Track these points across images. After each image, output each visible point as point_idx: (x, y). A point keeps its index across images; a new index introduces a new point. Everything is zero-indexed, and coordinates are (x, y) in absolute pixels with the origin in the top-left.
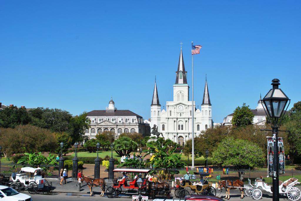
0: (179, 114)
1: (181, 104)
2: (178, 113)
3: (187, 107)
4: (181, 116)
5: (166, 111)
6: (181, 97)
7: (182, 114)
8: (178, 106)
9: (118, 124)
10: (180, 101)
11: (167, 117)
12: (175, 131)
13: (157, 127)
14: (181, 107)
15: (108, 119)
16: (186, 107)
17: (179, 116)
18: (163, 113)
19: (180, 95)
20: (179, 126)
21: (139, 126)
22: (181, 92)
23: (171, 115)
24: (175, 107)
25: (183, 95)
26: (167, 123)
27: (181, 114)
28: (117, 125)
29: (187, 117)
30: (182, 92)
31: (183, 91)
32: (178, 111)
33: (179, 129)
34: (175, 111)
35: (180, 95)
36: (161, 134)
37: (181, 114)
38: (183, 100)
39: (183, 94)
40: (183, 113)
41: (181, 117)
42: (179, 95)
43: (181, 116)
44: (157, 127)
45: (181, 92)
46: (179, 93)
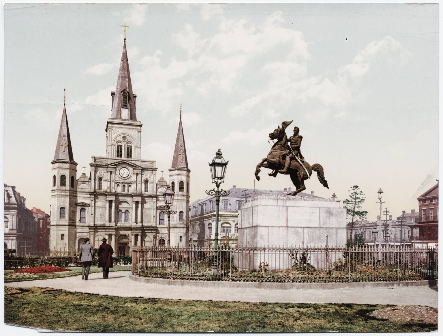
1: (124, 166)
2: (117, 184)
3: (139, 172)
4: (124, 190)
7: (127, 185)
13: (296, 131)
14: (124, 172)
24: (113, 170)
26: (93, 205)
27: (124, 186)
32: (117, 179)
37: (124, 186)
39: (129, 142)
40: (130, 184)
41: (126, 192)
42: (119, 144)
44: (296, 131)
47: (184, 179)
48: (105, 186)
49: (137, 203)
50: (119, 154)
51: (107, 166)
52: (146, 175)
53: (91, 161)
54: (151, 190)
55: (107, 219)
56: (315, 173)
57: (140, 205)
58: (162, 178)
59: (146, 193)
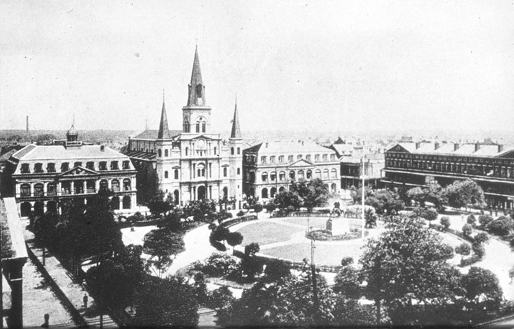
0: (199, 152)
2: (198, 151)
4: (201, 155)
5: (180, 149)
7: (203, 152)
10: (201, 133)
18: (177, 152)
22: (201, 119)
23: (187, 155)
27: (201, 153)
30: (203, 119)
31: (204, 117)
33: (199, 175)
37: (201, 153)
38: (204, 130)
43: (201, 155)
45: (201, 119)
46: (198, 119)
51: (191, 140)
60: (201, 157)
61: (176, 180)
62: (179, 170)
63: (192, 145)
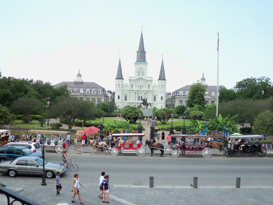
0: (140, 87)
1: (141, 79)
6: (141, 73)
7: (142, 87)
8: (139, 80)
9: (86, 94)
10: (141, 77)
11: (129, 89)
12: (136, 102)
13: (147, 99)
15: (77, 89)
16: (145, 81)
17: (139, 89)
19: (141, 71)
20: (139, 97)
21: (104, 96)
24: (136, 81)
25: (143, 71)
28: (86, 95)
29: (146, 90)
30: (142, 69)
31: (143, 68)
32: (138, 85)
33: (139, 100)
34: (137, 84)
35: (141, 71)
36: (149, 105)
44: (147, 99)
46: (140, 69)
47: (163, 84)
48: (134, 88)
49: (145, 93)
50: (139, 75)
52: (149, 83)
53: (129, 78)
54: (151, 89)
55: (134, 100)
56: (149, 105)
57: (146, 94)
58: (155, 83)
59: (149, 90)
60: (140, 90)
61: (126, 101)
62: (127, 95)
63: (135, 83)
